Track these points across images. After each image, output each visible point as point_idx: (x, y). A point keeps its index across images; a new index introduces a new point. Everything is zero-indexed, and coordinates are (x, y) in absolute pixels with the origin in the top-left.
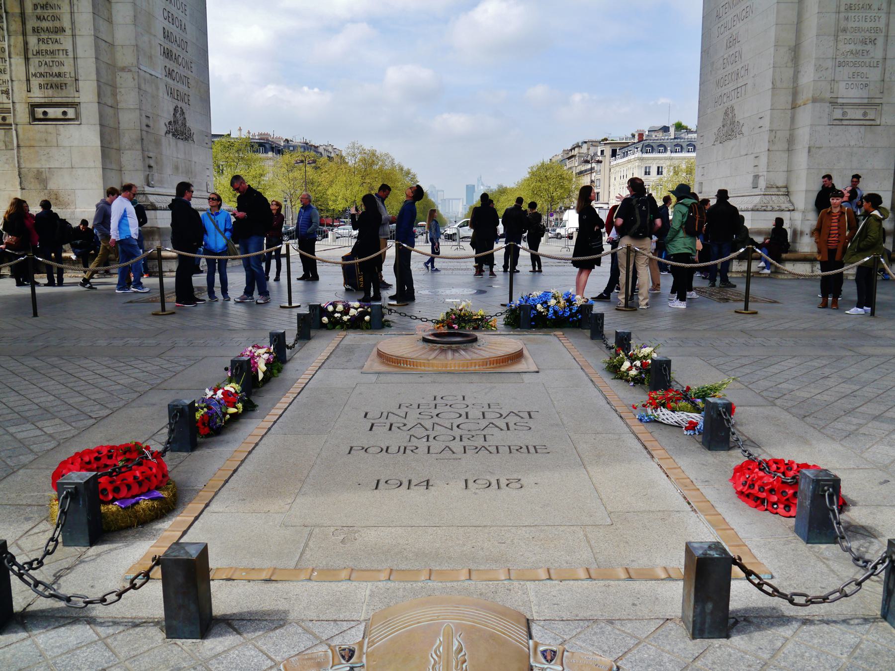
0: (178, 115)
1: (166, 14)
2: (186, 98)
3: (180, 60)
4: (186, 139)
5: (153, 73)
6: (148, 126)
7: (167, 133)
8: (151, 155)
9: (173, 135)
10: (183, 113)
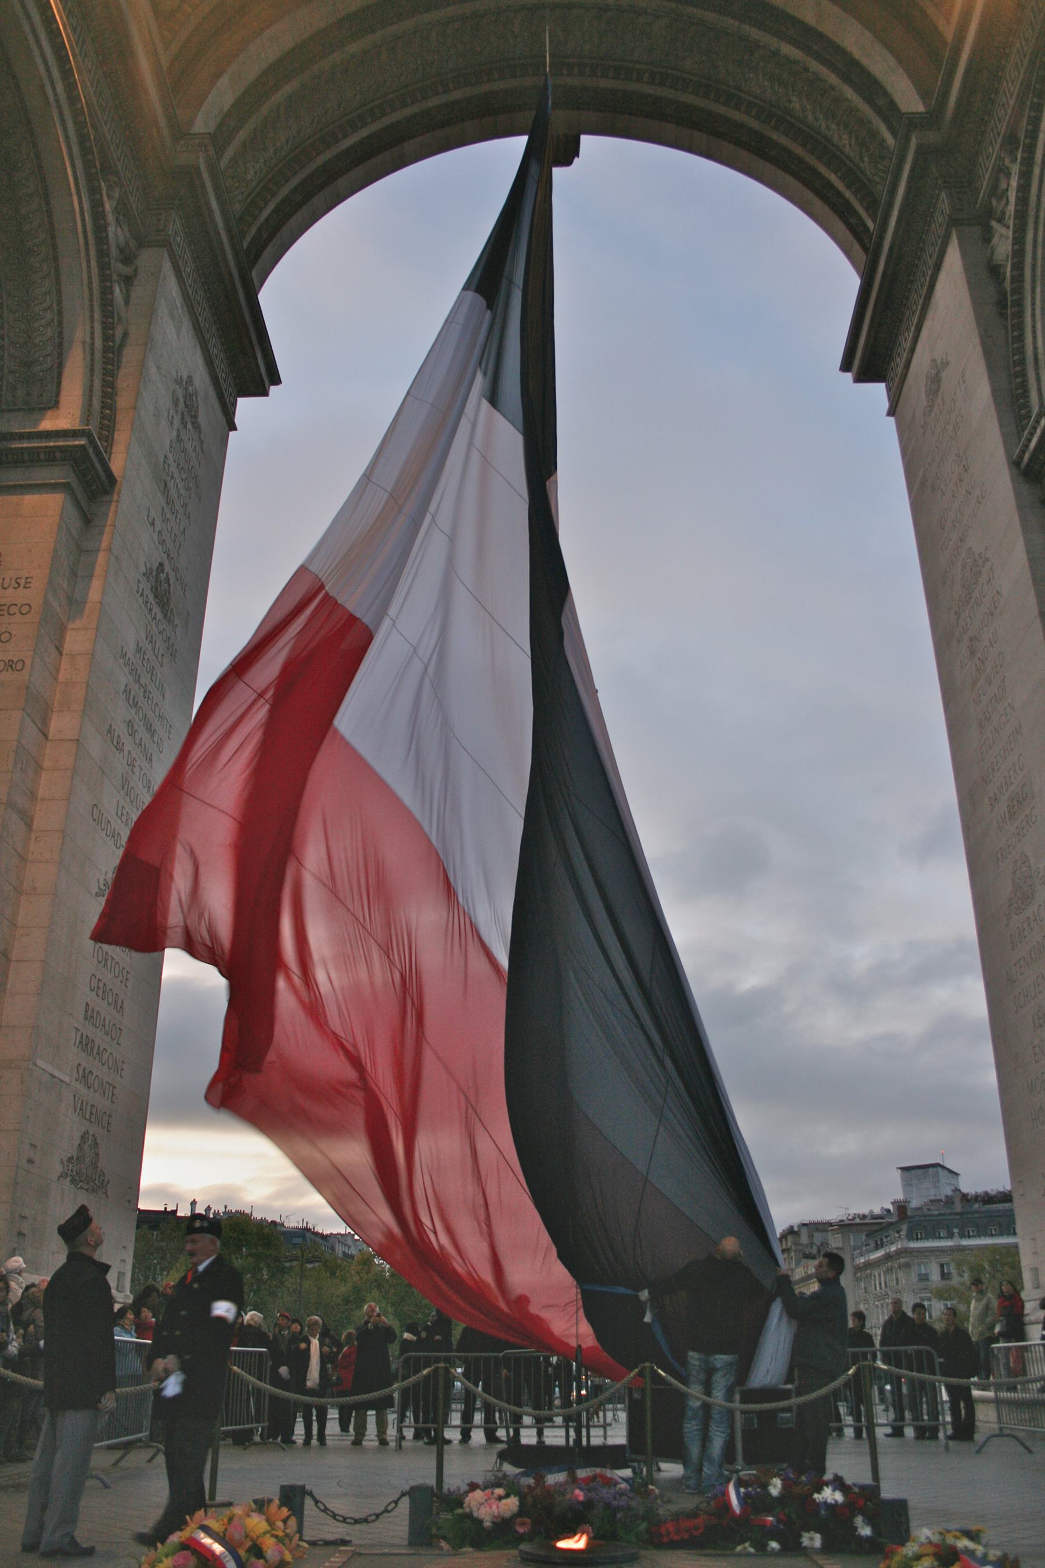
0: (86, 1147)
1: (94, 983)
2: (106, 1119)
3: (105, 1056)
4: (94, 1190)
5: (57, 1073)
6: (30, 1161)
7: (61, 1176)
8: (26, 1212)
9: (73, 1181)
10: (96, 1144)
